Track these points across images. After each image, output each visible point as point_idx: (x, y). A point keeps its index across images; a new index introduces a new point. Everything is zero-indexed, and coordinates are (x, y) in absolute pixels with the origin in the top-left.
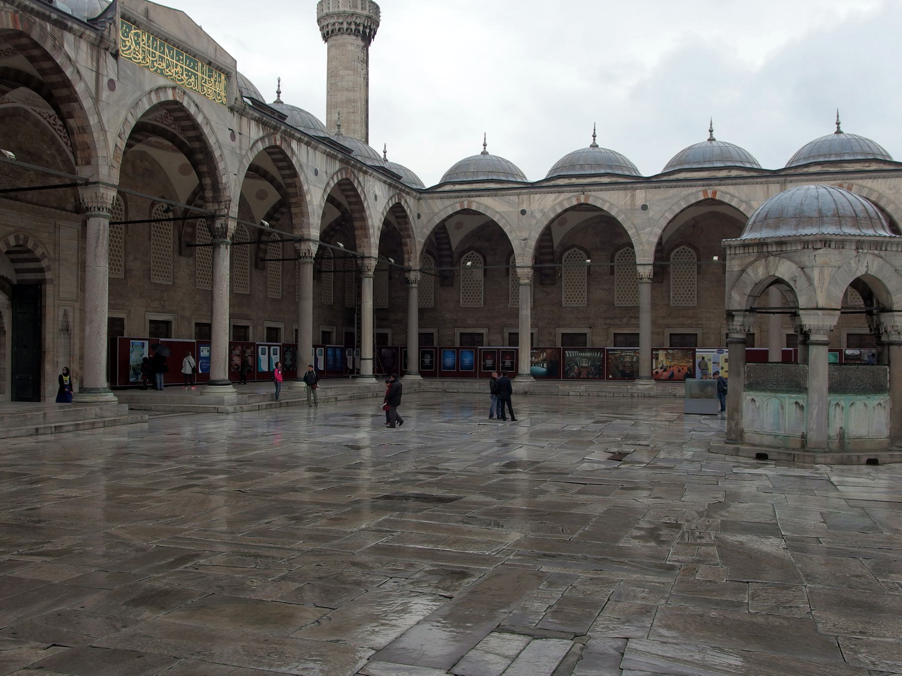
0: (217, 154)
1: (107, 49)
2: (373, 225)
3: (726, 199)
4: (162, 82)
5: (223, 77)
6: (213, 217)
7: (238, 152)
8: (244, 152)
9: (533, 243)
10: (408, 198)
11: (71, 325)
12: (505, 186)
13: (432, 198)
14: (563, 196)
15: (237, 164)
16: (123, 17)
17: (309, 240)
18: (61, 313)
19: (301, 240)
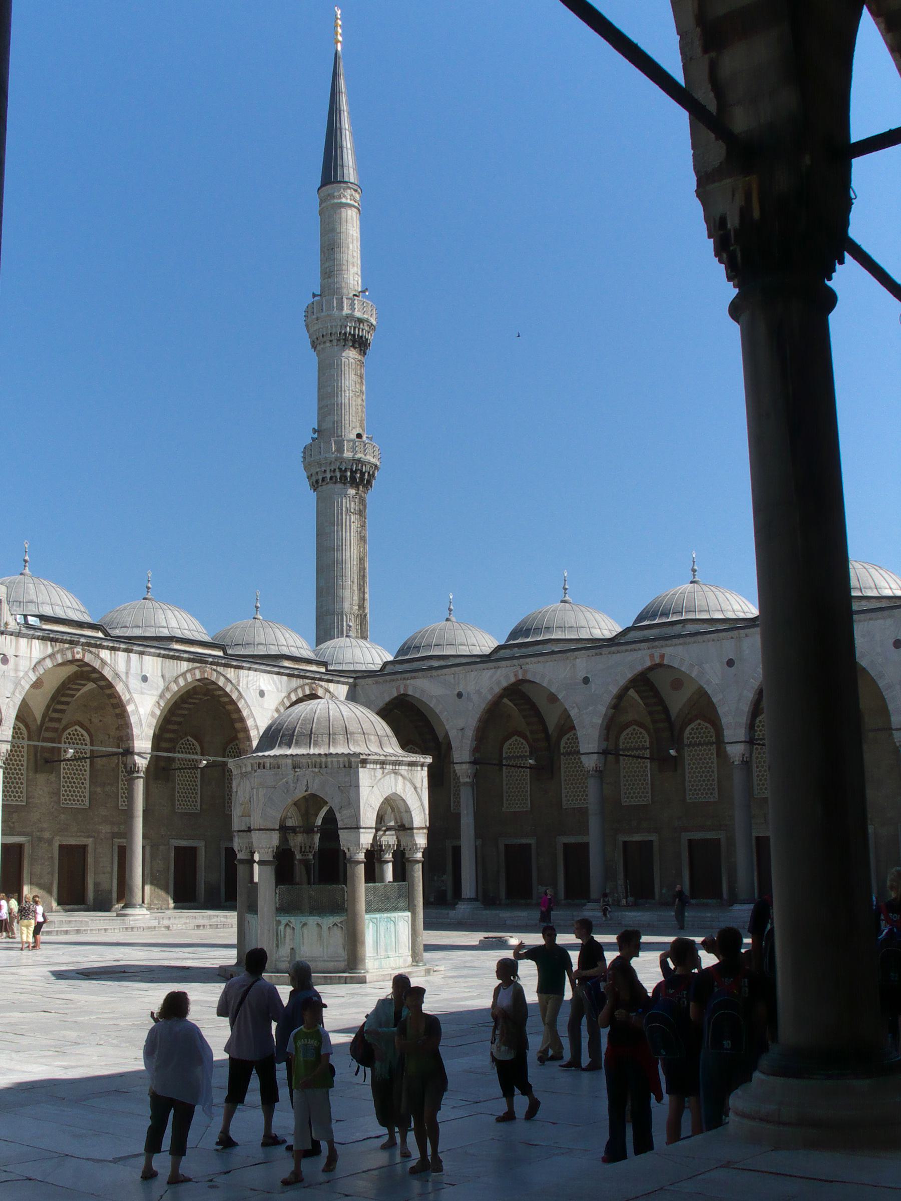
7: (12, 674)
9: (470, 733)
14: (499, 672)
15: (10, 686)
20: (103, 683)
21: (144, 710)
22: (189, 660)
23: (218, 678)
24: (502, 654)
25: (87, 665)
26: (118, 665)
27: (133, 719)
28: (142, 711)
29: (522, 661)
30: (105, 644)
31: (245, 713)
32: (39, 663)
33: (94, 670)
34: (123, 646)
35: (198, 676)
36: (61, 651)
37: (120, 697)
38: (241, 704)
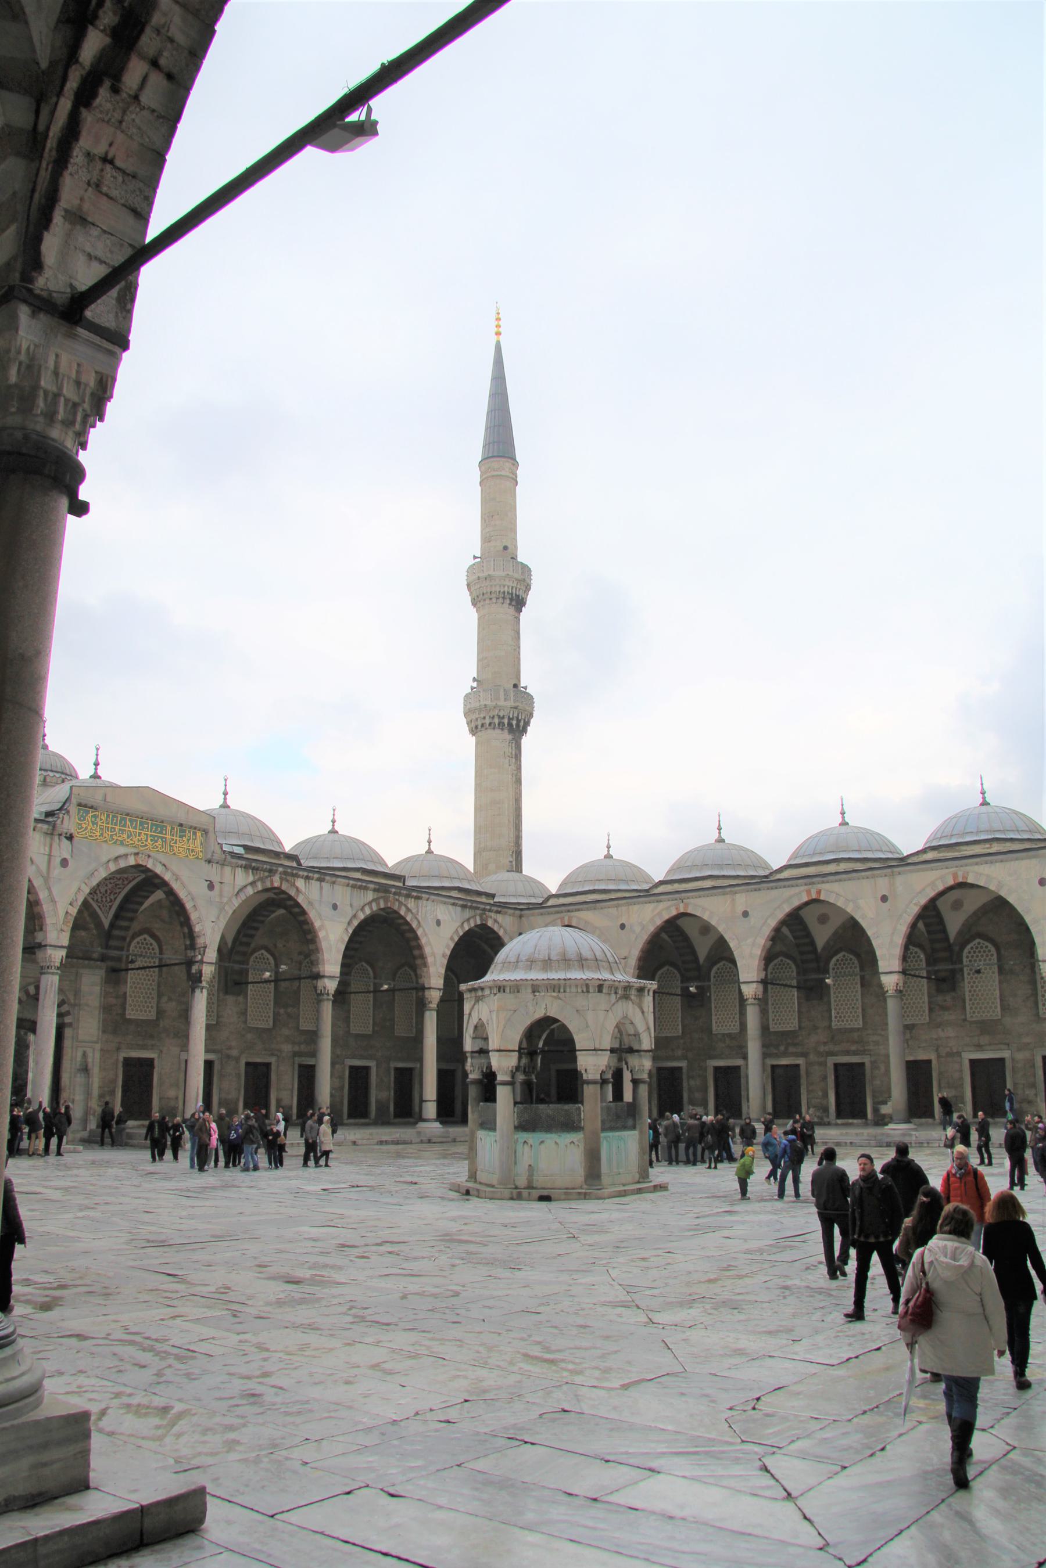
0: (189, 906)
1: (60, 835)
2: (433, 954)
3: (831, 899)
4: (122, 850)
5: (199, 834)
6: (190, 963)
7: (217, 900)
8: (225, 900)
10: (499, 918)
11: (90, 1065)
12: (613, 896)
13: (533, 915)
16: (79, 805)
17: (323, 977)
18: (80, 1054)
19: (318, 976)
20: (297, 910)
21: (333, 937)
22: (375, 890)
23: (399, 907)
24: (661, 889)
25: (284, 892)
26: (309, 894)
27: (324, 945)
28: (332, 937)
29: (683, 895)
30: (301, 873)
31: (423, 941)
32: (241, 890)
33: (290, 898)
34: (316, 876)
35: (382, 906)
36: (262, 879)
37: (312, 924)
38: (419, 932)
